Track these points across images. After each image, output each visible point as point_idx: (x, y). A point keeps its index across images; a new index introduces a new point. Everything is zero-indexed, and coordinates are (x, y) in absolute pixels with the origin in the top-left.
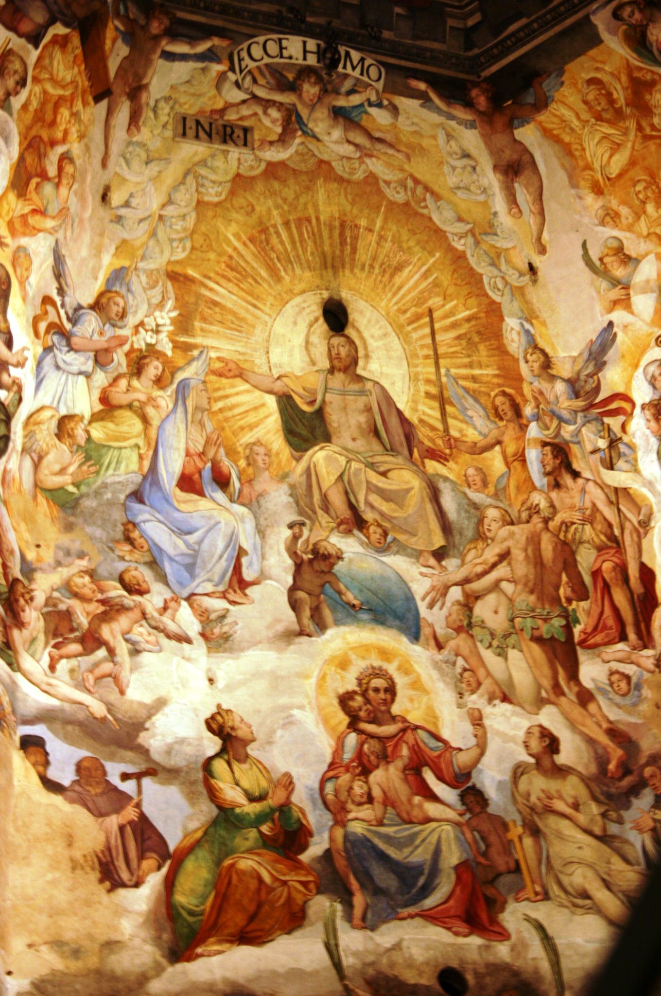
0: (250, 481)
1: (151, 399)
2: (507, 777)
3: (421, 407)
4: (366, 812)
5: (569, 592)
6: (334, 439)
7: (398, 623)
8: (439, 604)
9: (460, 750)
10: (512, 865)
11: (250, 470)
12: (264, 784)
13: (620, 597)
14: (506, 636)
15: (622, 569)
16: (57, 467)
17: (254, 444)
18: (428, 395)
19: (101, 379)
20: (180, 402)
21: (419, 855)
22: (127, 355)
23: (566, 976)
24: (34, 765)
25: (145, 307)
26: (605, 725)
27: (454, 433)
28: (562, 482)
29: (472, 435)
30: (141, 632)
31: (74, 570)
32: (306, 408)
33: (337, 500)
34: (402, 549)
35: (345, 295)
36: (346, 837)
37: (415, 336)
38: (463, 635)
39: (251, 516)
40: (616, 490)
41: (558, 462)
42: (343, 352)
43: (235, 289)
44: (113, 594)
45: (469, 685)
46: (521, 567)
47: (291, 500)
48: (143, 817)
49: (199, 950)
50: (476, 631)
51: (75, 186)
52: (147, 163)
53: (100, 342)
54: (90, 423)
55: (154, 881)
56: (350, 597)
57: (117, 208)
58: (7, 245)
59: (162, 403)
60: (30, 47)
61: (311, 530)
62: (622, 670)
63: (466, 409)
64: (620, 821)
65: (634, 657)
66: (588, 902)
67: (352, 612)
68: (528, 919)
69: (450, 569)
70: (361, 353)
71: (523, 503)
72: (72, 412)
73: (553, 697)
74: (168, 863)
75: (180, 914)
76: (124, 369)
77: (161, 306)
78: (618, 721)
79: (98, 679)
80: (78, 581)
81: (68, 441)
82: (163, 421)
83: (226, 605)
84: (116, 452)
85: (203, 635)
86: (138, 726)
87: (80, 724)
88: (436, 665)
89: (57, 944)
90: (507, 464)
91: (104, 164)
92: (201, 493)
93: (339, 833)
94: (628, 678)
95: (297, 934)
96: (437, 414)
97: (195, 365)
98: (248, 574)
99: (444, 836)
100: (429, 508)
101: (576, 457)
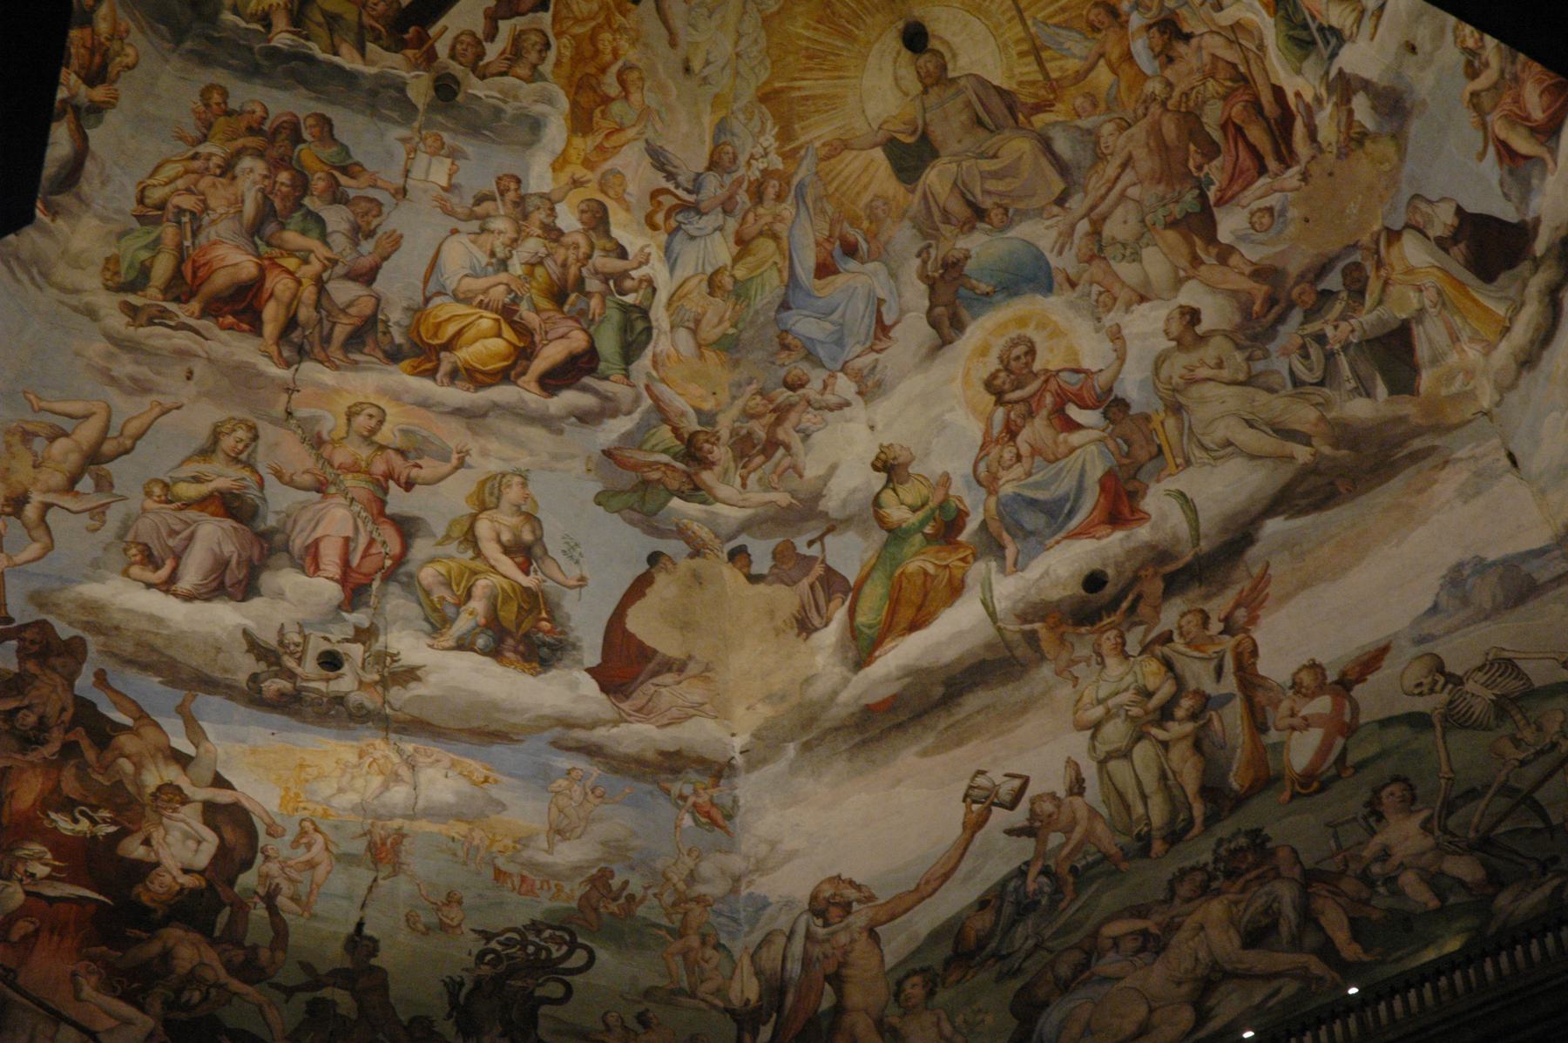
0: (875, 236)
1: (778, 218)
2: (1148, 373)
3: (1017, 71)
4: (1018, 470)
5: (1199, 158)
6: (942, 153)
7: (1031, 285)
8: (1068, 246)
9: (1101, 371)
10: (1154, 450)
11: (874, 227)
12: (925, 491)
13: (1256, 134)
14: (1138, 240)
15: (1256, 105)
16: (716, 320)
17: (872, 201)
18: (1022, 54)
19: (732, 224)
20: (801, 204)
21: (1066, 485)
22: (747, 191)
23: (1203, 529)
24: (740, 569)
25: (750, 139)
26: (1248, 270)
27: (1054, 75)
28: (1171, 53)
29: (1073, 65)
30: (809, 418)
31: (747, 396)
32: (910, 140)
33: (957, 207)
34: (1024, 215)
35: (918, 12)
36: (998, 503)
37: (994, 7)
38: (1096, 263)
39: (883, 266)
40: (1232, 26)
41: (1166, 36)
42: (931, 67)
43: (820, 74)
44: (780, 400)
45: (1105, 305)
46: (1146, 163)
47: (914, 231)
48: (828, 569)
49: (877, 653)
50: (1108, 252)
51: (648, 84)
52: (710, 17)
53: (722, 193)
54: (733, 267)
55: (840, 615)
56: (984, 287)
57: (701, 71)
58: (588, 181)
59: (786, 214)
60: (540, 14)
61: (937, 248)
62: (1262, 206)
63: (1061, 44)
64: (1266, 356)
65: (1277, 185)
66: (1230, 449)
67: (988, 299)
68: (1169, 493)
69: (1074, 206)
70: (948, 56)
71: (1137, 101)
72: (716, 267)
73: (1191, 272)
74: (850, 595)
75: (862, 632)
76: (749, 204)
77: (762, 131)
78: (1261, 259)
79: (780, 476)
80: (752, 403)
81: (719, 293)
82: (791, 230)
83: (874, 356)
84: (759, 280)
85: (860, 393)
86: (818, 496)
87: (773, 519)
88: (1072, 305)
89: (768, 698)
90: (1114, 71)
91: (673, 44)
92: (836, 272)
93: (993, 500)
94: (1270, 210)
95: (959, 603)
96: (1035, 67)
97: (805, 163)
98: (888, 320)
99: (1088, 458)
100: (1044, 162)
101: (1185, 19)
